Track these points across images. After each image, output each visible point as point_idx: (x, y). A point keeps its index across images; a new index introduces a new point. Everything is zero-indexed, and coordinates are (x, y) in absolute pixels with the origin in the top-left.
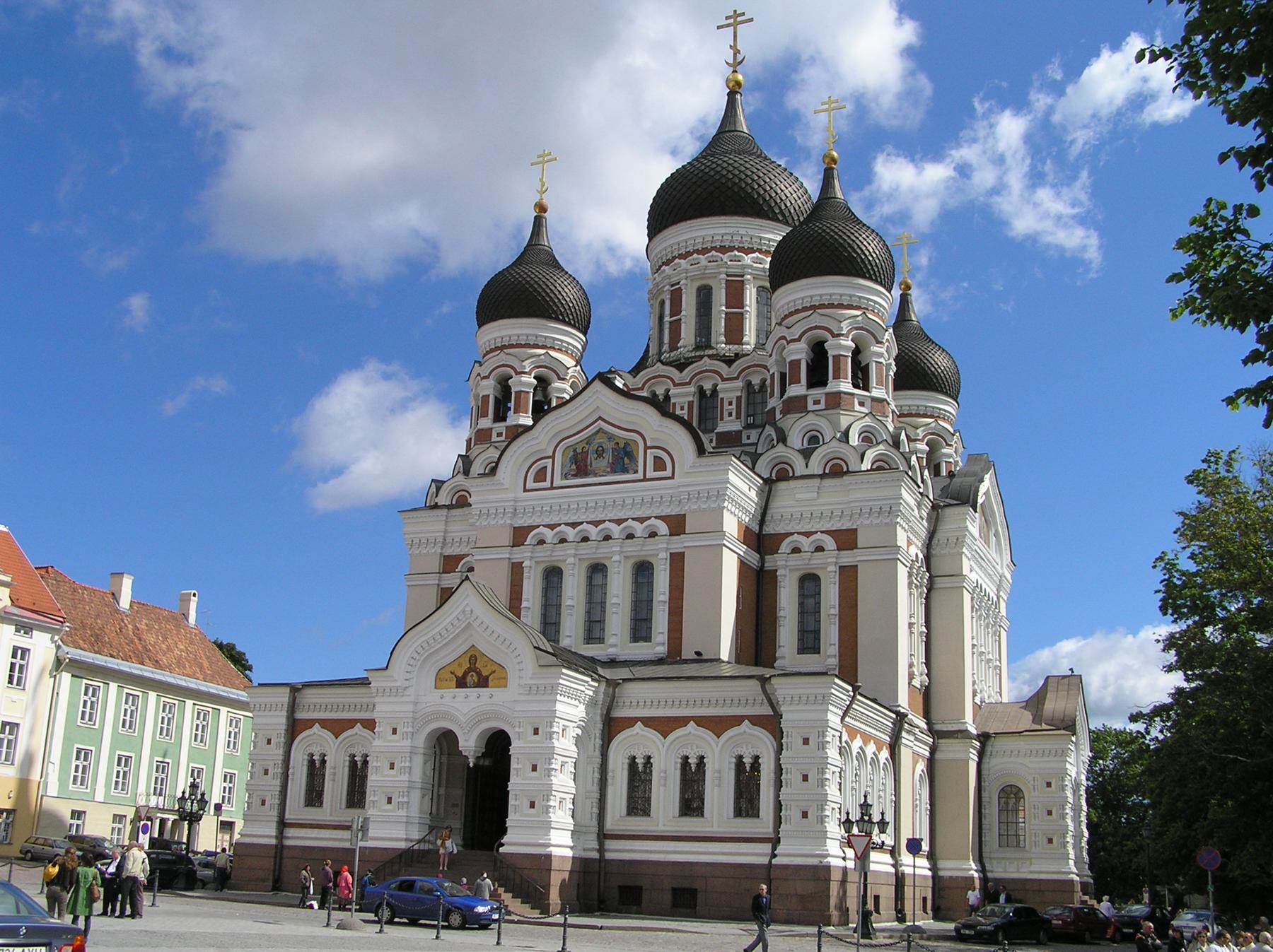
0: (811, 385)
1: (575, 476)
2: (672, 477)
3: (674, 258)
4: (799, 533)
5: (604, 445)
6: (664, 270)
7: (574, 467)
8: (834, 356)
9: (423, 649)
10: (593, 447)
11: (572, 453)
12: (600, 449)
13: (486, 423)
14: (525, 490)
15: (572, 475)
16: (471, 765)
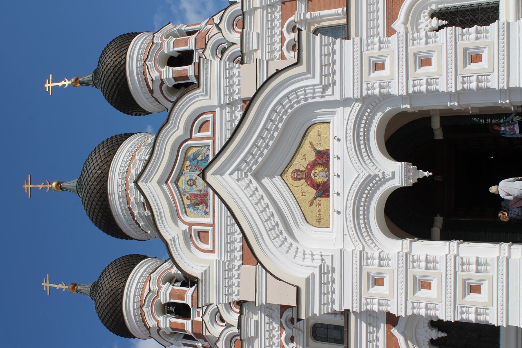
0: (190, 64)
1: (207, 204)
2: (214, 113)
3: (130, 209)
4: (282, 46)
5: (188, 178)
6: (136, 215)
7: (200, 207)
8: (174, 47)
9: (278, 236)
10: (187, 188)
11: (191, 209)
12: (189, 183)
13: (188, 325)
14: (213, 251)
15: (207, 208)
16: (426, 174)
